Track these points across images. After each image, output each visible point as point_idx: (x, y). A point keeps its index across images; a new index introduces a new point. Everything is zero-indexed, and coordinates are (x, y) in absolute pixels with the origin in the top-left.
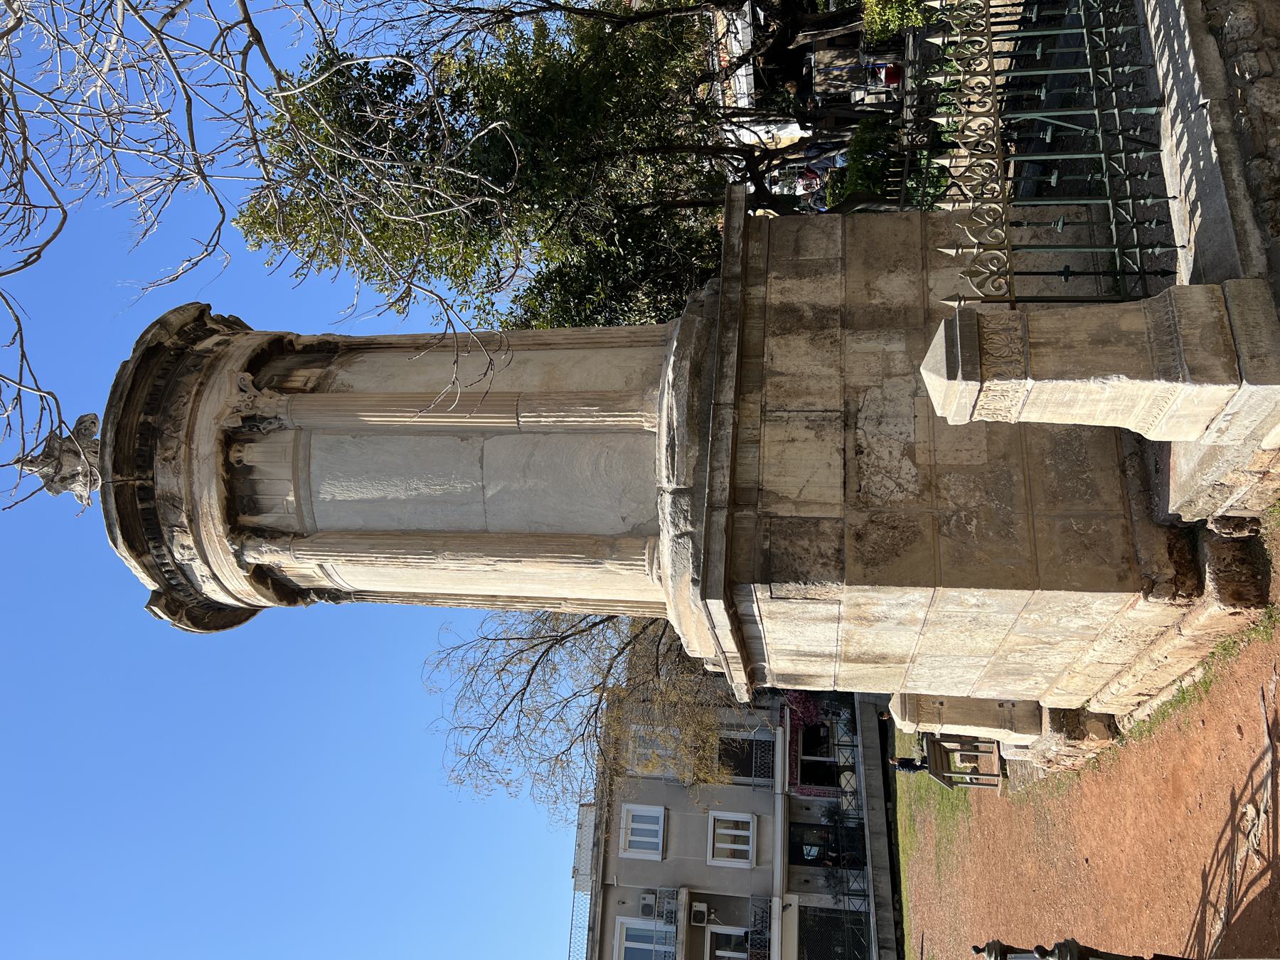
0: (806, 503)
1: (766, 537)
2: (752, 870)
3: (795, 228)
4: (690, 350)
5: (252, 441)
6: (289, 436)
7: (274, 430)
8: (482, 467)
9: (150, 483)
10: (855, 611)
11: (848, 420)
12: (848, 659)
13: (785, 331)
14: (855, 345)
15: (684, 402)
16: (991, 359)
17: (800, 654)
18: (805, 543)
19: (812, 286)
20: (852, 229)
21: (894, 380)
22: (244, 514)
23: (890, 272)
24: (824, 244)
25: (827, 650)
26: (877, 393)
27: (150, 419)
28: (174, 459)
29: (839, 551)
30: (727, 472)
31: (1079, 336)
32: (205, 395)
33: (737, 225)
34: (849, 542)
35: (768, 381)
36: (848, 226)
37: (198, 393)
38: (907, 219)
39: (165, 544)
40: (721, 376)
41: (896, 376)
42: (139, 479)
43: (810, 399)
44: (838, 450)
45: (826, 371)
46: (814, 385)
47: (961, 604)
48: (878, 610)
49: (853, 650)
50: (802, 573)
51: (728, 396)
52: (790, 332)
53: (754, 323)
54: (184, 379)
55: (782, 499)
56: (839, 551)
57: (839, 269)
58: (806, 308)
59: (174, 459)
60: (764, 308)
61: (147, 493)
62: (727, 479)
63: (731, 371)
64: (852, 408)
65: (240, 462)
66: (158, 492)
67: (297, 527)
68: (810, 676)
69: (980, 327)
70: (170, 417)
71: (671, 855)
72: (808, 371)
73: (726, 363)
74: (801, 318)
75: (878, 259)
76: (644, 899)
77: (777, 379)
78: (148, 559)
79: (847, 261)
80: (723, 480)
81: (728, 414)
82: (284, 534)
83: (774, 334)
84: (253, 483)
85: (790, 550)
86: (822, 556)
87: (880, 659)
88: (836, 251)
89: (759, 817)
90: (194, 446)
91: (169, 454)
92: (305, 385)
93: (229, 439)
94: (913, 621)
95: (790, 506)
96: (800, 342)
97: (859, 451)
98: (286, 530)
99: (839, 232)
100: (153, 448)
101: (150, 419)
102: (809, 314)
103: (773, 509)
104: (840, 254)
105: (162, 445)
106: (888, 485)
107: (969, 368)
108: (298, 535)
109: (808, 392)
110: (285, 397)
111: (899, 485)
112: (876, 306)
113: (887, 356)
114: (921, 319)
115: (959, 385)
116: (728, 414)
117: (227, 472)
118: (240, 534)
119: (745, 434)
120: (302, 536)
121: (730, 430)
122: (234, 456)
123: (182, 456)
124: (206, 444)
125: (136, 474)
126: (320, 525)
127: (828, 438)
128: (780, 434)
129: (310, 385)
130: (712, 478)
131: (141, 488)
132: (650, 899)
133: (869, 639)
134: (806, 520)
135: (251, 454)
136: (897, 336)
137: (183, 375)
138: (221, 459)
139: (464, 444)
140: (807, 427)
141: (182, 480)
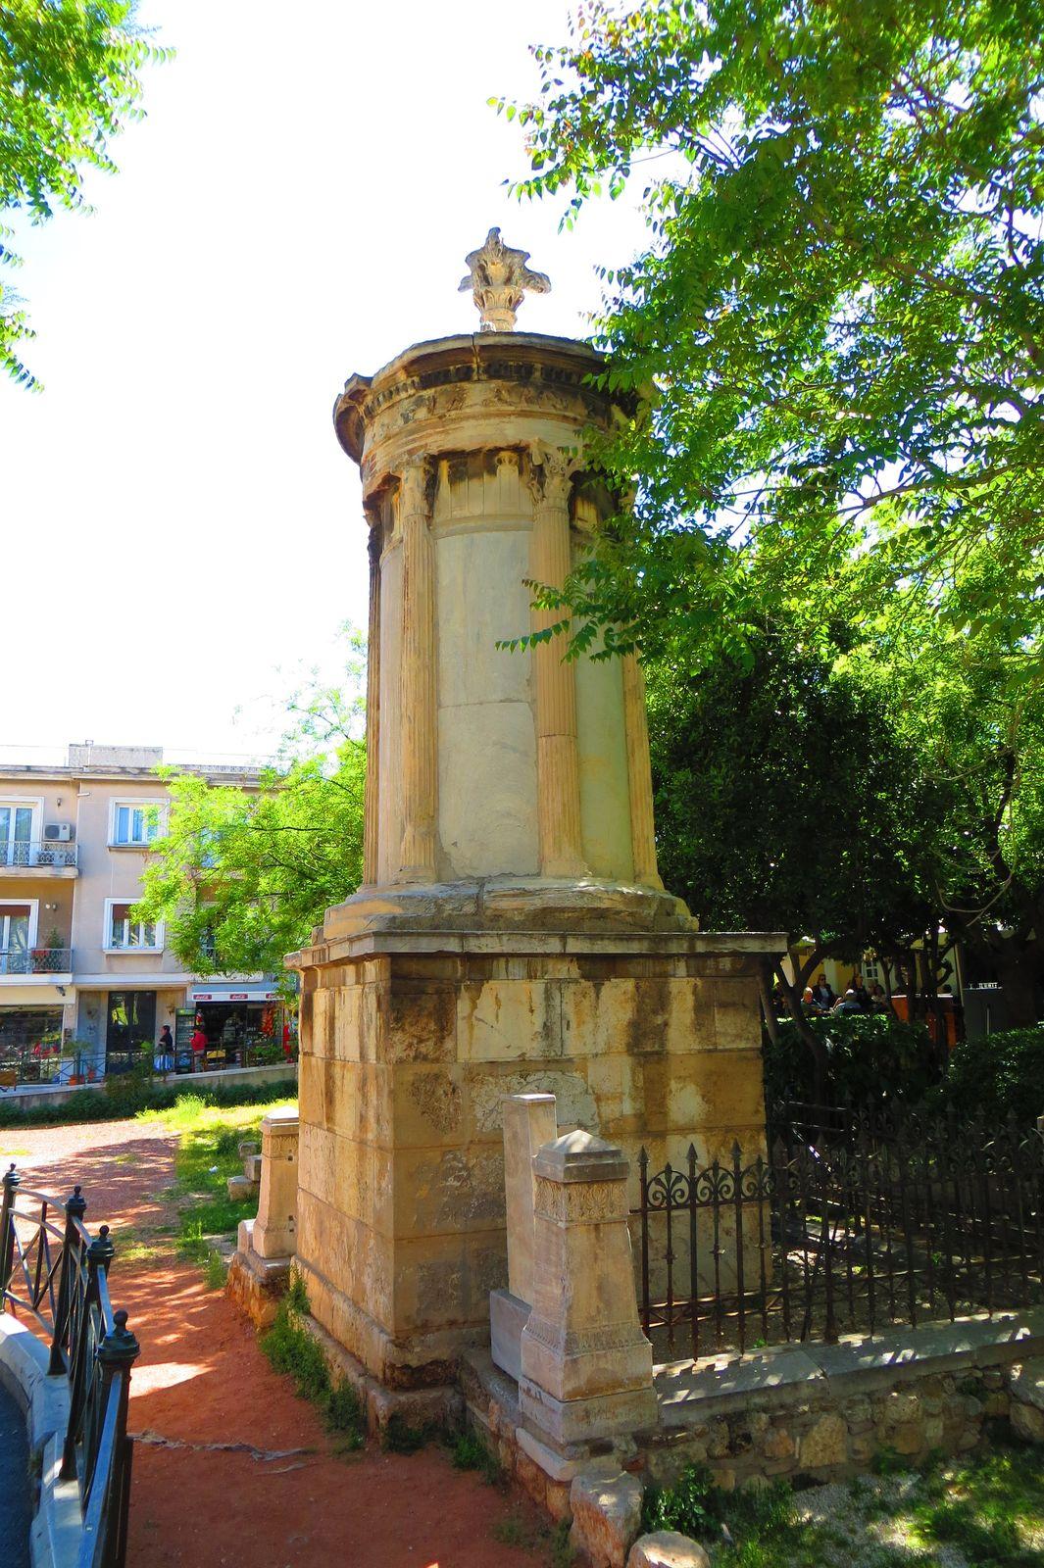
0: (472, 1027)
2: (101, 950)
3: (746, 1002)
5: (521, 472)
6: (528, 509)
8: (501, 701)
9: (476, 378)
15: (567, 904)
16: (584, 1192)
17: (331, 1021)
18: (432, 1026)
20: (745, 1058)
22: (450, 467)
23: (703, 1097)
24: (732, 1030)
27: (537, 374)
29: (425, 1058)
32: (565, 425)
34: (435, 1068)
37: (565, 418)
38: (757, 1112)
40: (592, 937)
42: (478, 368)
43: (573, 1025)
44: (524, 1054)
45: (602, 1038)
49: (337, 1071)
50: (403, 1024)
51: (575, 946)
53: (651, 967)
54: (580, 401)
56: (425, 1058)
57: (706, 1047)
59: (500, 399)
60: (665, 976)
61: (466, 375)
66: (466, 385)
67: (438, 519)
68: (312, 1028)
69: (613, 1181)
70: (541, 393)
71: (115, 856)
73: (606, 942)
74: (655, 1012)
75: (715, 1083)
76: (65, 828)
78: (402, 377)
79: (714, 1054)
80: (488, 945)
81: (554, 946)
83: (637, 987)
84: (478, 475)
88: (724, 1043)
89: (160, 955)
90: (512, 417)
92: (579, 519)
93: (520, 450)
99: (742, 1045)
100: (509, 378)
101: (537, 374)
102: (659, 1020)
103: (464, 995)
104: (721, 1047)
105: (513, 387)
106: (490, 1103)
108: (429, 518)
110: (564, 504)
111: (492, 1111)
112: (668, 1085)
116: (554, 946)
117: (489, 450)
118: (430, 463)
119: (538, 964)
120: (429, 526)
122: (505, 455)
123: (503, 408)
124: (512, 431)
125: (482, 364)
126: (441, 542)
127: (535, 1044)
129: (579, 524)
131: (470, 370)
132: (64, 835)
135: (507, 472)
137: (583, 399)
138: (503, 444)
141: (478, 409)
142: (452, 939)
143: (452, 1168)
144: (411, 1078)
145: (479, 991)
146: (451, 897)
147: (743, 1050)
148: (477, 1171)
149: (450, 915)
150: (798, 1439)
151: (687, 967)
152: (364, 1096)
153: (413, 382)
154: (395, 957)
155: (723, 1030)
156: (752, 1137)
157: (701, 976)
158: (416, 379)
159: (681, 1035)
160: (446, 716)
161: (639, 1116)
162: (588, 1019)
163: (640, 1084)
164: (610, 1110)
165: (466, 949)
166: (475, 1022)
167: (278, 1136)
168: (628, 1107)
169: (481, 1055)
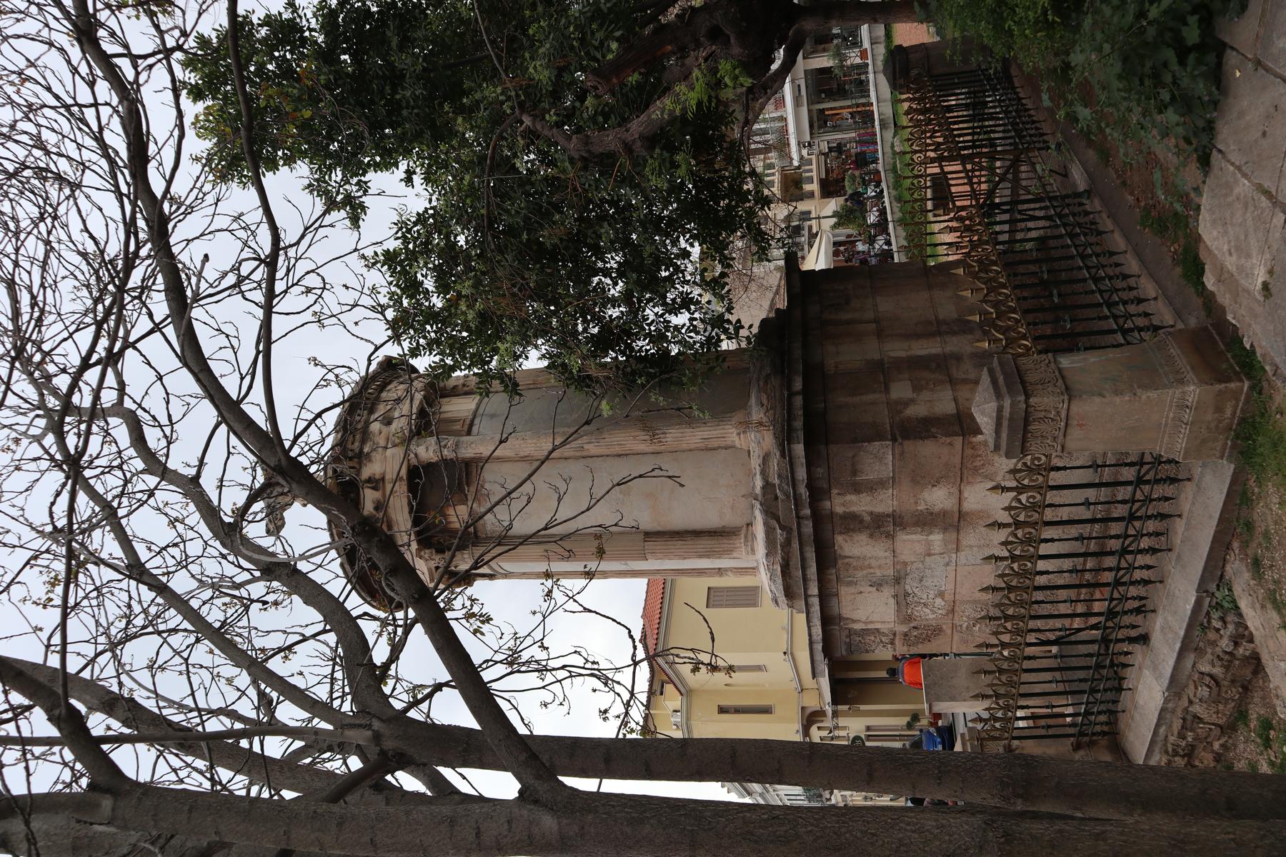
0: (872, 622)
3: (850, 454)
4: (779, 558)
13: (847, 531)
14: (905, 537)
19: (869, 498)
20: (902, 453)
23: (934, 486)
29: (893, 639)
35: (840, 562)
36: (897, 452)
38: (951, 444)
43: (872, 571)
45: (882, 554)
52: (853, 530)
72: (869, 555)
73: (808, 573)
74: (862, 521)
83: (841, 533)
96: (862, 538)
97: (907, 594)
99: (890, 457)
103: (851, 626)
109: (870, 567)
113: (929, 543)
114: (956, 519)
128: (852, 590)
136: (937, 531)
143: (967, 628)
147: (893, 455)
151: (821, 500)
156: (973, 448)
159: (884, 502)
161: (945, 530)
162: (866, 563)
163: (920, 530)
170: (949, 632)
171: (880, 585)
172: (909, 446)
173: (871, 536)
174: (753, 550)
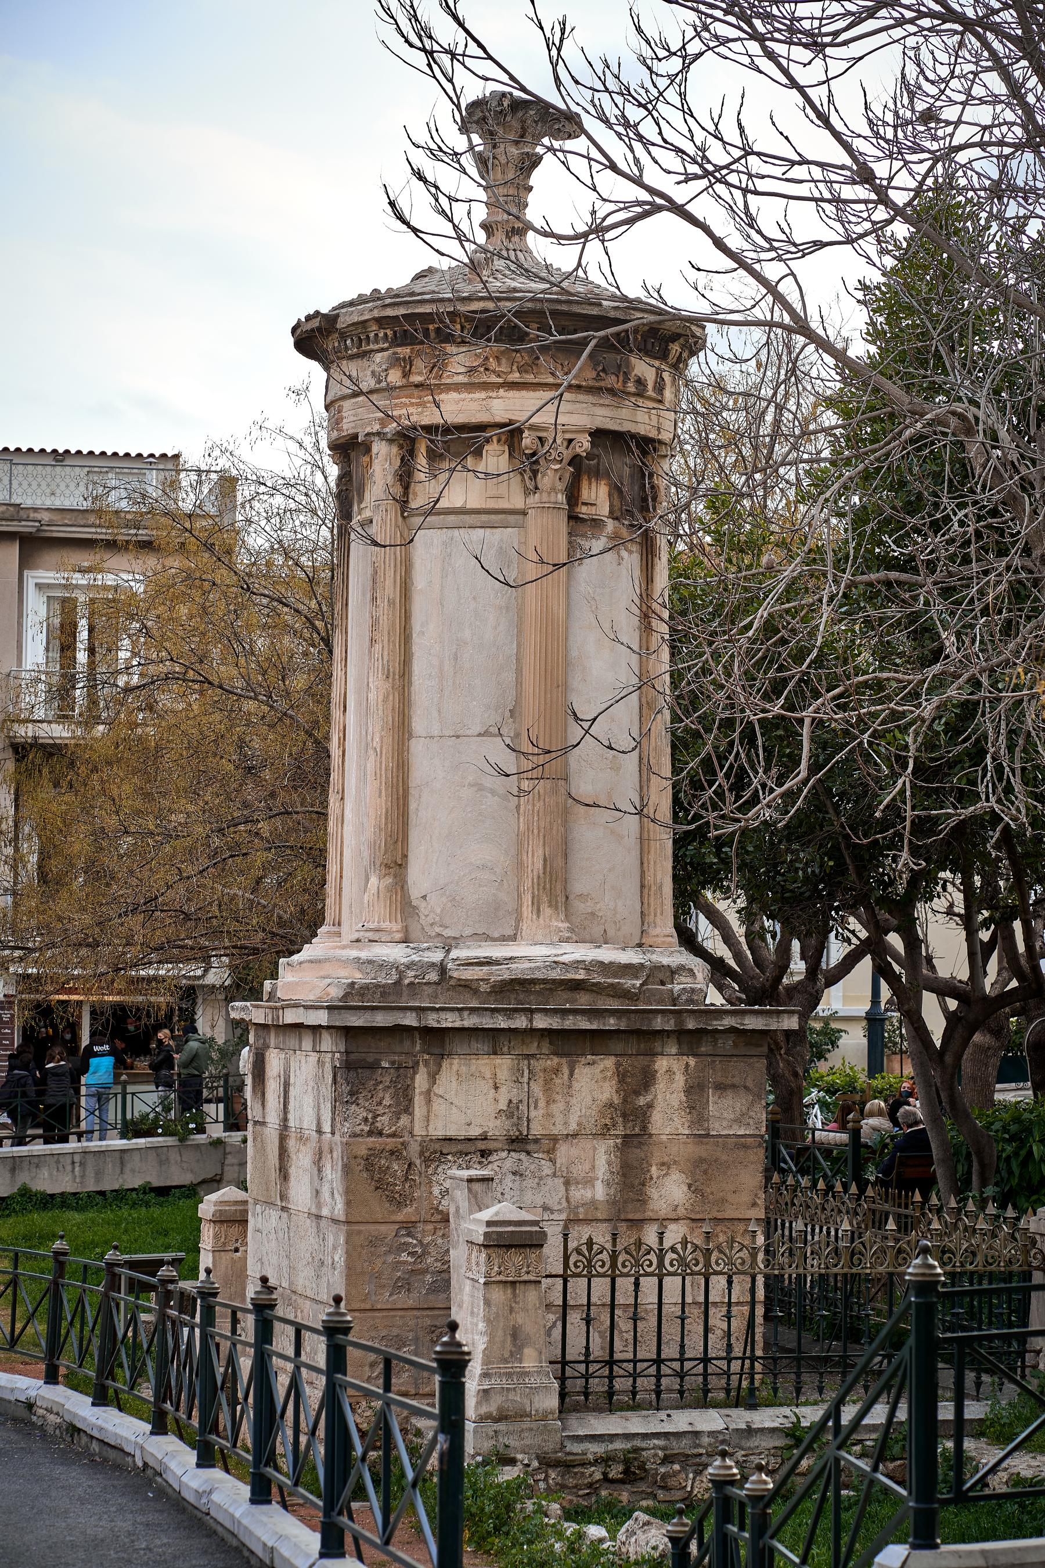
0: (429, 1101)
1: (393, 1063)
3: (750, 1083)
4: (597, 979)
7: (523, 480)
8: (479, 735)
10: (326, 1148)
11: (518, 1142)
12: (283, 1139)
13: (622, 1077)
15: (538, 975)
17: (287, 1085)
18: (387, 1101)
20: (745, 1147)
21: (563, 1188)
23: (690, 1186)
24: (729, 1115)
25: (291, 1116)
26: (547, 1169)
28: (486, 369)
29: (380, 1134)
30: (457, 1024)
31: (520, 1319)
33: (746, 1022)
35: (564, 1060)
39: (390, 347)
41: (567, 1190)
43: (542, 1104)
46: (557, 1108)
47: (335, 1248)
48: (328, 1171)
49: (292, 1144)
51: (541, 1022)
55: (433, 1078)
58: (649, 1098)
62: (450, 1025)
63: (570, 1023)
64: (531, 1147)
65: (488, 441)
68: (263, 1094)
72: (573, 1101)
73: (579, 1018)
74: (637, 1093)
75: (705, 1172)
77: (566, 1071)
80: (450, 1021)
82: (406, 488)
83: (618, 1065)
85: (381, 1087)
86: (375, 1117)
87: (284, 1174)
91: (493, 363)
94: (319, 1206)
95: (425, 1086)
96: (608, 1092)
98: (411, 491)
105: (502, 353)
107: (494, 1236)
108: (403, 503)
113: (590, 1182)
114: (630, 1216)
115: (482, 1229)
119: (503, 1040)
121: (503, 1025)
127: (498, 1122)
128: (503, 1074)
130: (452, 1009)
133: (301, 1160)
134: (411, 1100)
136: (612, 1191)
139: (507, 714)
140: (510, 1101)
141: (461, 379)
142: (409, 1014)
144: (364, 1152)
145: (440, 1066)
146: (413, 963)
148: (431, 1249)
149: (411, 984)
150: (691, 1476)
151: (680, 1043)
152: (320, 1171)
153: (386, 334)
154: (348, 1032)
155: (718, 1115)
157: (694, 1055)
158: (389, 333)
160: (418, 748)
161: (612, 1203)
162: (558, 1097)
164: (580, 1194)
165: (423, 1023)
166: (434, 1098)
167: (222, 1222)
168: (600, 1192)
169: (438, 1129)
170: (400, 1217)
171: (510, 1115)
172: (758, 1157)
173: (610, 1105)
174: (567, 940)
